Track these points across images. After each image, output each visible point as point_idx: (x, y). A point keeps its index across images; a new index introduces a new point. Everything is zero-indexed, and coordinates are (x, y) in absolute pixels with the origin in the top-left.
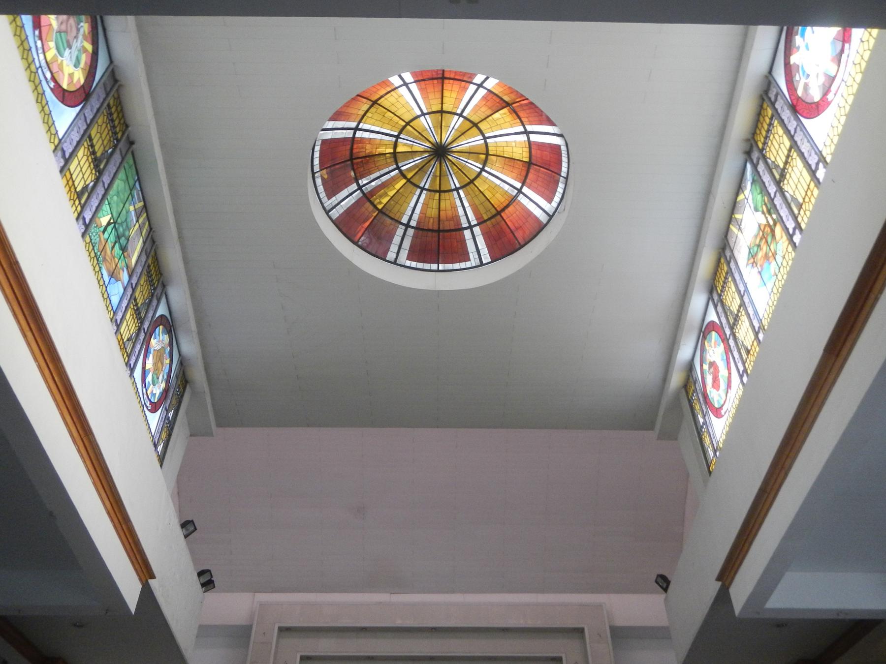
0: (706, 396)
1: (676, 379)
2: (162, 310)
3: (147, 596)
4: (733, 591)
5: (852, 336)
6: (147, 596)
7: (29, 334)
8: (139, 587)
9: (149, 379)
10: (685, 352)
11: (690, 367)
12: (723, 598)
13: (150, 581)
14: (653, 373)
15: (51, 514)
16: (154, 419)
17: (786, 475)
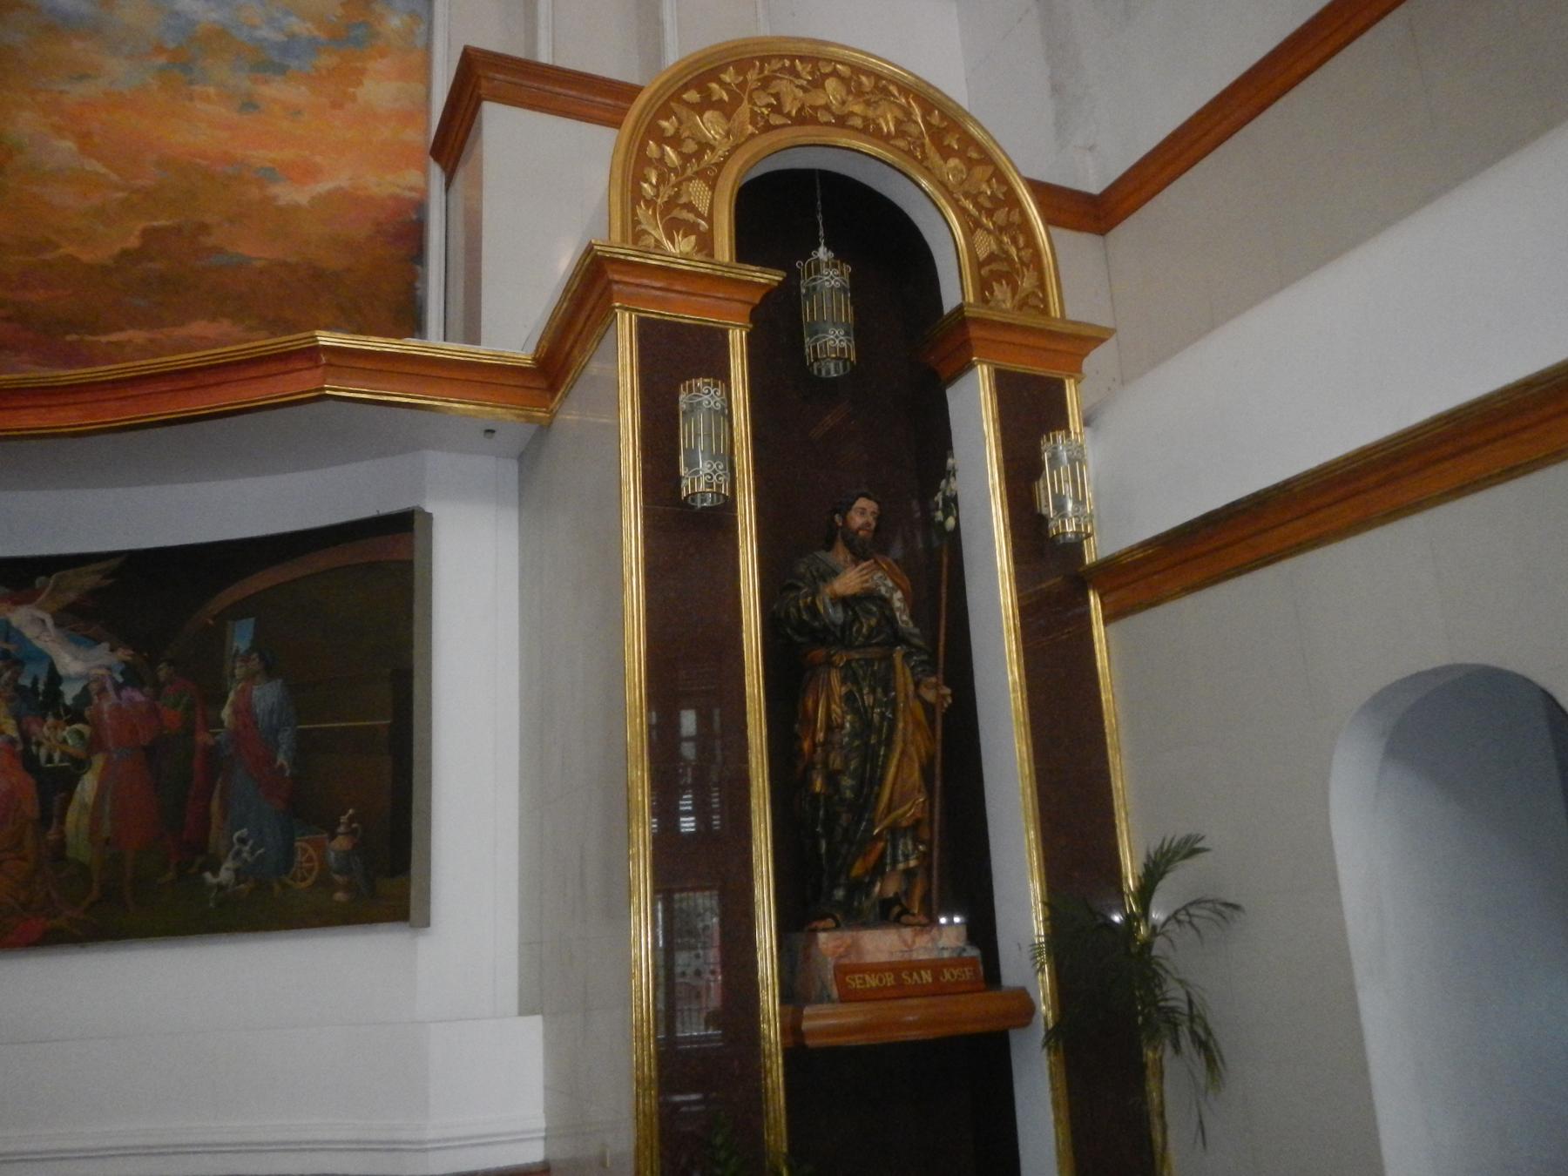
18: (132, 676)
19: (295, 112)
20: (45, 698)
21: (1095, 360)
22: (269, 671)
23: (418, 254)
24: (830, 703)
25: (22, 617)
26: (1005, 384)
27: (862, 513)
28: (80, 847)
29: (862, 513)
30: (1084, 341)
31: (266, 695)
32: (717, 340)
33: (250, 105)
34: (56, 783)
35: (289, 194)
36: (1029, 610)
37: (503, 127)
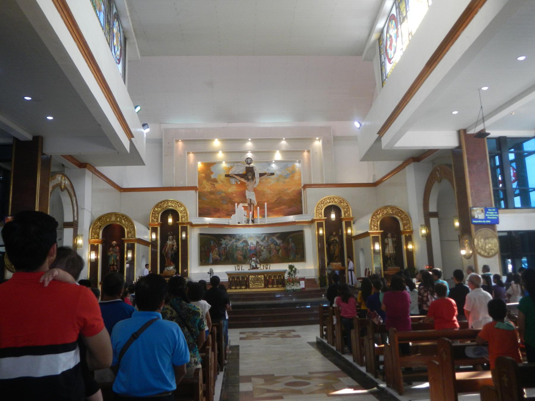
0: (386, 50)
1: (374, 36)
2: (115, 11)
3: (132, 145)
4: (383, 139)
5: (436, 63)
6: (132, 145)
7: (90, 65)
8: (129, 142)
9: (116, 49)
10: (380, 25)
11: (382, 31)
12: (379, 140)
13: (132, 139)
14: (364, 33)
15: (99, 125)
16: (120, 66)
17: (407, 104)
18: (283, 243)
19: (288, 182)
20: (276, 244)
21: (354, 219)
22: (293, 242)
23: (301, 196)
24: (332, 247)
25: (274, 238)
26: (346, 222)
27: (334, 233)
28: (280, 256)
29: (334, 233)
30: (352, 219)
31: (293, 244)
32: (322, 223)
33: (284, 182)
34: (278, 251)
35: (289, 191)
36: (347, 239)
37: (308, 190)
